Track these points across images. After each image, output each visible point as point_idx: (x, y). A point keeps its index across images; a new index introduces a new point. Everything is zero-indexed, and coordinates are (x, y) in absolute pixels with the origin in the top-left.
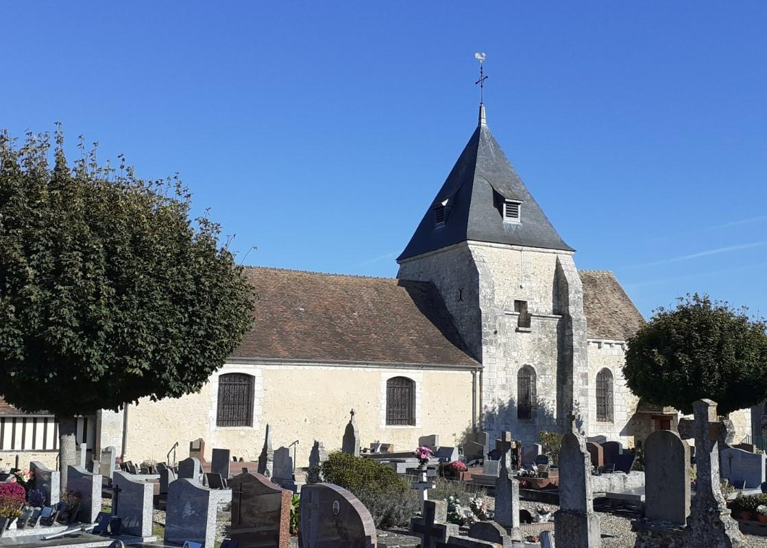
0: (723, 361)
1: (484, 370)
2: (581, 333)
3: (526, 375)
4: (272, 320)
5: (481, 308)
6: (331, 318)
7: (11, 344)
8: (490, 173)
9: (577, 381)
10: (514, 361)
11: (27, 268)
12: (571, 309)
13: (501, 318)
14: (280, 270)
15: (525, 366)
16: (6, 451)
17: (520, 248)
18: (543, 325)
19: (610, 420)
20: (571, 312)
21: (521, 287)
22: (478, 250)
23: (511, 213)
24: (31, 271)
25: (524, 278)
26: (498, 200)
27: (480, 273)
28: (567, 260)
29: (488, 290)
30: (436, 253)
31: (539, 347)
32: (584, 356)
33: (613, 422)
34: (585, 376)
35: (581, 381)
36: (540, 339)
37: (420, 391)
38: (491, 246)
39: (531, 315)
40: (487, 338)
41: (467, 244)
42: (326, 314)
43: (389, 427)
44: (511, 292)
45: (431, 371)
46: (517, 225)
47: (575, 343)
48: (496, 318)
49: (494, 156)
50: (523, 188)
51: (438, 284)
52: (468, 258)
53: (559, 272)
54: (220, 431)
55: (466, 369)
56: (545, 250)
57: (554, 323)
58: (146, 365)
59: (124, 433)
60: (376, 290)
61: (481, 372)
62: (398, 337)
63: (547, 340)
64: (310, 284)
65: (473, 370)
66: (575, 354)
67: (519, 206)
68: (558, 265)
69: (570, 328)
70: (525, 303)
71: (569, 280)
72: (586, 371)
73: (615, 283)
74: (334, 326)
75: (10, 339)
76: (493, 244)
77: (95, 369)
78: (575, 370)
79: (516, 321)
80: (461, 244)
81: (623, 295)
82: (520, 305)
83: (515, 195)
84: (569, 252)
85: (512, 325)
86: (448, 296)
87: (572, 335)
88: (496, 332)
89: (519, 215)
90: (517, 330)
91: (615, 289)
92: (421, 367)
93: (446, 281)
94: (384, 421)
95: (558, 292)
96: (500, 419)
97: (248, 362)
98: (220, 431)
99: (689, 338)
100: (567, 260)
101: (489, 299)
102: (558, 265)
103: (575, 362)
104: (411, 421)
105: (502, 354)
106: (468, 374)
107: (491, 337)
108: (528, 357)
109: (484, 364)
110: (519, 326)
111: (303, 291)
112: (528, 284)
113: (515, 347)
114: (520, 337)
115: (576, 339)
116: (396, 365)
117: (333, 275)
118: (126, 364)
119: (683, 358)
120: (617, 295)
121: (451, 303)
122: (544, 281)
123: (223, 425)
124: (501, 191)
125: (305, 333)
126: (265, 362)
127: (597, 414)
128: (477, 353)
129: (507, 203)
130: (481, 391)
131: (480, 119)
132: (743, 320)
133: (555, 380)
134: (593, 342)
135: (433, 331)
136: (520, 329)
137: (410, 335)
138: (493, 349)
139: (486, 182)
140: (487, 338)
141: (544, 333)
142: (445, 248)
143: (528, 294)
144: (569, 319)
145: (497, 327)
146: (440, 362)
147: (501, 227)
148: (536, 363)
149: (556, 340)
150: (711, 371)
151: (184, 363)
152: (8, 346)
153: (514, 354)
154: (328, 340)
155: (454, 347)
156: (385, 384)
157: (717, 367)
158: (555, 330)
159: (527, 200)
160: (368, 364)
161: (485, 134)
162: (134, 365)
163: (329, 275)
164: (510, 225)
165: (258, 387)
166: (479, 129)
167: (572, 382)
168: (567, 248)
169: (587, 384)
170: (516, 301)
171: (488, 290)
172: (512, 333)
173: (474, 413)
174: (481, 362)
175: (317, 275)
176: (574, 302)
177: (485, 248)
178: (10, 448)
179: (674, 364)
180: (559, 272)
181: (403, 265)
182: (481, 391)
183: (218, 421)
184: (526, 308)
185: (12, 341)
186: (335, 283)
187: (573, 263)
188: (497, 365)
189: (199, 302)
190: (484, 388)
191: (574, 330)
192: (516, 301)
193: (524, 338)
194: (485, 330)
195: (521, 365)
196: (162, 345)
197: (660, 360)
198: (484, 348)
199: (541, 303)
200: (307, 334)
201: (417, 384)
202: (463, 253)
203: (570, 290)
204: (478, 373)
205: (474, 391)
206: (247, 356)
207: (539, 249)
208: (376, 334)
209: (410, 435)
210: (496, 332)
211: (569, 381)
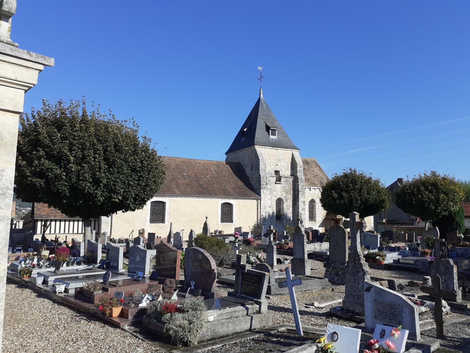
0: (362, 196)
1: (262, 200)
3: (279, 202)
4: (173, 179)
6: (197, 178)
7: (64, 189)
8: (264, 117)
9: (301, 204)
11: (71, 157)
12: (298, 174)
14: (176, 158)
15: (279, 198)
16: (61, 234)
17: (277, 148)
18: (287, 181)
19: (314, 221)
20: (298, 175)
21: (277, 165)
22: (260, 150)
24: (72, 158)
25: (278, 161)
26: (268, 128)
28: (296, 153)
29: (263, 166)
31: (284, 190)
32: (304, 194)
33: (316, 222)
34: (304, 202)
36: (285, 187)
37: (235, 209)
38: (265, 148)
39: (281, 177)
41: (255, 147)
42: (195, 176)
43: (222, 223)
44: (273, 167)
45: (240, 200)
46: (276, 139)
47: (300, 188)
48: (267, 178)
49: (266, 110)
50: (278, 123)
51: (242, 163)
54: (151, 225)
56: (287, 149)
57: (291, 180)
58: (120, 198)
59: (111, 226)
60: (217, 166)
61: (261, 200)
62: (226, 186)
64: (189, 163)
65: (257, 200)
66: (300, 193)
68: (293, 156)
69: (298, 182)
70: (279, 171)
71: (297, 162)
72: (304, 200)
73: (316, 163)
74: (199, 181)
75: (63, 187)
77: (99, 199)
78: (300, 200)
79: (275, 179)
80: (252, 147)
81: (320, 168)
82: (277, 172)
84: (297, 150)
85: (273, 181)
86: (247, 169)
87: (299, 185)
88: (267, 184)
90: (276, 183)
92: (236, 198)
93: (246, 162)
94: (220, 221)
95: (293, 167)
97: (163, 196)
98: (151, 225)
99: (348, 186)
100: (296, 153)
102: (293, 156)
103: (300, 196)
104: (231, 221)
106: (255, 201)
107: (265, 186)
108: (280, 194)
109: (262, 197)
110: (276, 181)
111: (186, 166)
112: (280, 164)
113: (275, 190)
115: (300, 187)
116: (225, 198)
118: (112, 197)
119: (345, 195)
120: (317, 168)
123: (152, 223)
124: (269, 125)
125: (187, 184)
126: (170, 196)
128: (259, 193)
129: (271, 129)
130: (260, 208)
131: (260, 94)
133: (291, 204)
135: (240, 183)
136: (277, 182)
137: (231, 185)
138: (265, 191)
139: (263, 121)
141: (287, 184)
142: (246, 149)
144: (297, 178)
145: (267, 182)
146: (243, 196)
147: (269, 140)
148: (284, 197)
149: (292, 187)
150: (357, 200)
151: (136, 197)
152: (63, 189)
153: (274, 193)
154: (196, 187)
156: (220, 205)
158: (292, 183)
159: (280, 128)
160: (213, 197)
161: (262, 101)
162: (115, 198)
163: (197, 160)
164: (273, 139)
165: (167, 207)
166: (260, 98)
168: (297, 149)
169: (305, 206)
170: (275, 171)
171: (263, 166)
172: (273, 184)
173: (258, 218)
174: (260, 196)
175: (192, 160)
176: (300, 171)
177: (262, 148)
178: (63, 233)
179: (341, 197)
181: (228, 156)
182: (260, 208)
183: (150, 221)
184: (279, 174)
185: (64, 187)
186: (199, 163)
189: (143, 171)
191: (299, 183)
192: (275, 171)
193: (278, 186)
194: (262, 183)
195: (277, 197)
196: (127, 189)
197: (335, 195)
198: (262, 190)
199: (286, 172)
200: (187, 184)
201: (234, 206)
202: (253, 150)
203: (298, 166)
204: (259, 201)
205: (258, 208)
206: (163, 194)
208: (216, 185)
209: (231, 227)
210: (267, 184)
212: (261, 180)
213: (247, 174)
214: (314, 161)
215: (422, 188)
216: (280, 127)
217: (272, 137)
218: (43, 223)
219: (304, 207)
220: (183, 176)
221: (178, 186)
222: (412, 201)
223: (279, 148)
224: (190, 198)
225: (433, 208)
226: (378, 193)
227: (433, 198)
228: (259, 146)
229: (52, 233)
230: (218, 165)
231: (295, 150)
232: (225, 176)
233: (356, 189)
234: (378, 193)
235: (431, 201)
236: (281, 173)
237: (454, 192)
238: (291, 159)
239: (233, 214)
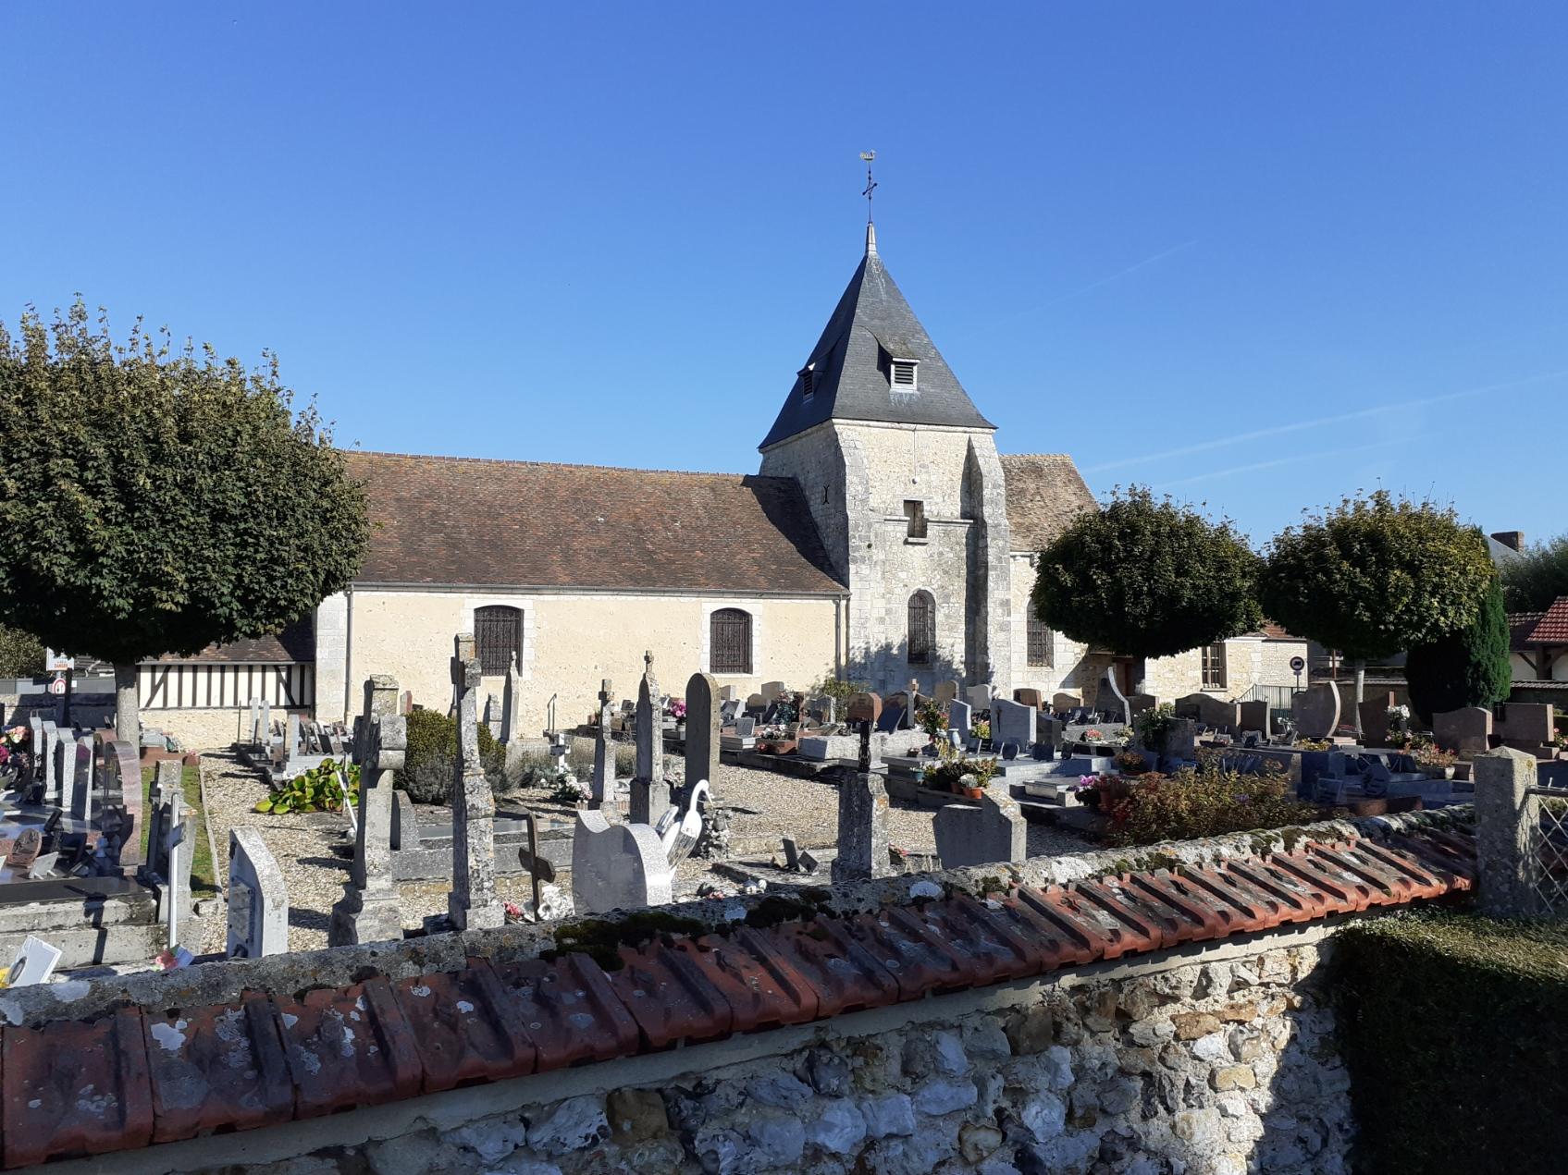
1: (852, 597)
2: (1001, 543)
3: (921, 605)
5: (849, 513)
6: (641, 531)
8: (876, 322)
9: (994, 612)
10: (901, 585)
12: (987, 511)
13: (877, 525)
15: (919, 591)
16: (200, 708)
17: (913, 426)
18: (946, 533)
20: (986, 514)
21: (914, 482)
22: (846, 430)
23: (905, 378)
26: (884, 360)
27: (847, 463)
28: (985, 442)
29: (860, 488)
30: (800, 438)
31: (939, 564)
32: (1005, 575)
34: (1006, 604)
35: (999, 611)
36: (941, 554)
38: (869, 426)
39: (928, 521)
40: (856, 554)
41: (833, 424)
44: (899, 490)
47: (990, 558)
48: (870, 525)
50: (926, 341)
52: (833, 442)
53: (971, 459)
55: (826, 596)
57: (962, 531)
58: (180, 598)
60: (713, 490)
61: (848, 600)
63: (951, 555)
64: (617, 485)
65: (836, 598)
66: (990, 573)
67: (915, 368)
68: (970, 449)
69: (985, 537)
71: (984, 469)
72: (1007, 597)
76: (871, 423)
77: (112, 603)
79: (906, 529)
80: (826, 424)
81: (1082, 487)
82: (913, 507)
83: (909, 352)
84: (987, 430)
86: (813, 497)
87: (987, 547)
88: (869, 546)
89: (915, 380)
90: (906, 542)
91: (1070, 481)
92: (761, 595)
93: (812, 476)
95: (970, 487)
96: (876, 664)
99: (1108, 548)
100: (985, 442)
101: (862, 500)
102: (970, 449)
103: (991, 584)
104: (747, 668)
105: (879, 575)
106: (829, 605)
107: (864, 552)
108: (924, 579)
109: (852, 590)
110: (910, 536)
112: (925, 477)
113: (903, 566)
114: (912, 552)
116: (723, 593)
117: (652, 472)
119: (1100, 578)
120: (1072, 488)
121: (816, 507)
122: (950, 471)
124: (890, 347)
127: (1029, 655)
129: (896, 363)
130: (848, 627)
131: (867, 244)
132: (1192, 521)
133: (963, 610)
134: (1022, 556)
135: (785, 545)
136: (911, 540)
138: (865, 570)
139: (869, 335)
140: (856, 554)
141: (947, 546)
142: (809, 430)
143: (924, 491)
144: (984, 525)
145: (872, 538)
148: (935, 586)
149: (964, 554)
153: (903, 575)
154: (631, 560)
155: (813, 568)
156: (708, 618)
157: (1145, 589)
158: (964, 540)
159: (930, 358)
161: (873, 267)
162: (164, 599)
164: (901, 395)
165: (528, 624)
166: (866, 258)
167: (987, 613)
168: (984, 424)
169: (1009, 615)
171: (860, 488)
172: (899, 547)
173: (838, 658)
177: (859, 428)
178: (205, 705)
179: (1086, 584)
180: (971, 459)
182: (848, 627)
184: (922, 511)
187: (993, 445)
188: (871, 591)
189: (255, 517)
190: (852, 622)
191: (989, 540)
192: (906, 502)
193: (917, 553)
194: (853, 542)
195: (913, 590)
196: (199, 572)
197: (1067, 579)
198: (852, 567)
199: (944, 503)
200: (603, 552)
202: (829, 436)
203: (984, 484)
204: (843, 603)
205: (838, 626)
206: (511, 583)
207: (941, 427)
210: (869, 546)
211: (983, 610)
212: (851, 533)
213: (814, 515)
214: (1064, 464)
215: (1332, 551)
216: (932, 353)
217: (897, 388)
218: (284, 674)
219: (1008, 619)
220: (594, 524)
221: (568, 559)
222: (1297, 593)
223: (919, 426)
224: (606, 597)
225: (1366, 617)
226: (1220, 569)
227: (1366, 582)
228: (849, 421)
229: (169, 705)
230: (716, 486)
231: (978, 430)
232: (735, 523)
233: (1136, 560)
234: (1220, 569)
235: (1361, 593)
236: (926, 507)
237: (1443, 559)
238: (963, 461)
239: (754, 643)
